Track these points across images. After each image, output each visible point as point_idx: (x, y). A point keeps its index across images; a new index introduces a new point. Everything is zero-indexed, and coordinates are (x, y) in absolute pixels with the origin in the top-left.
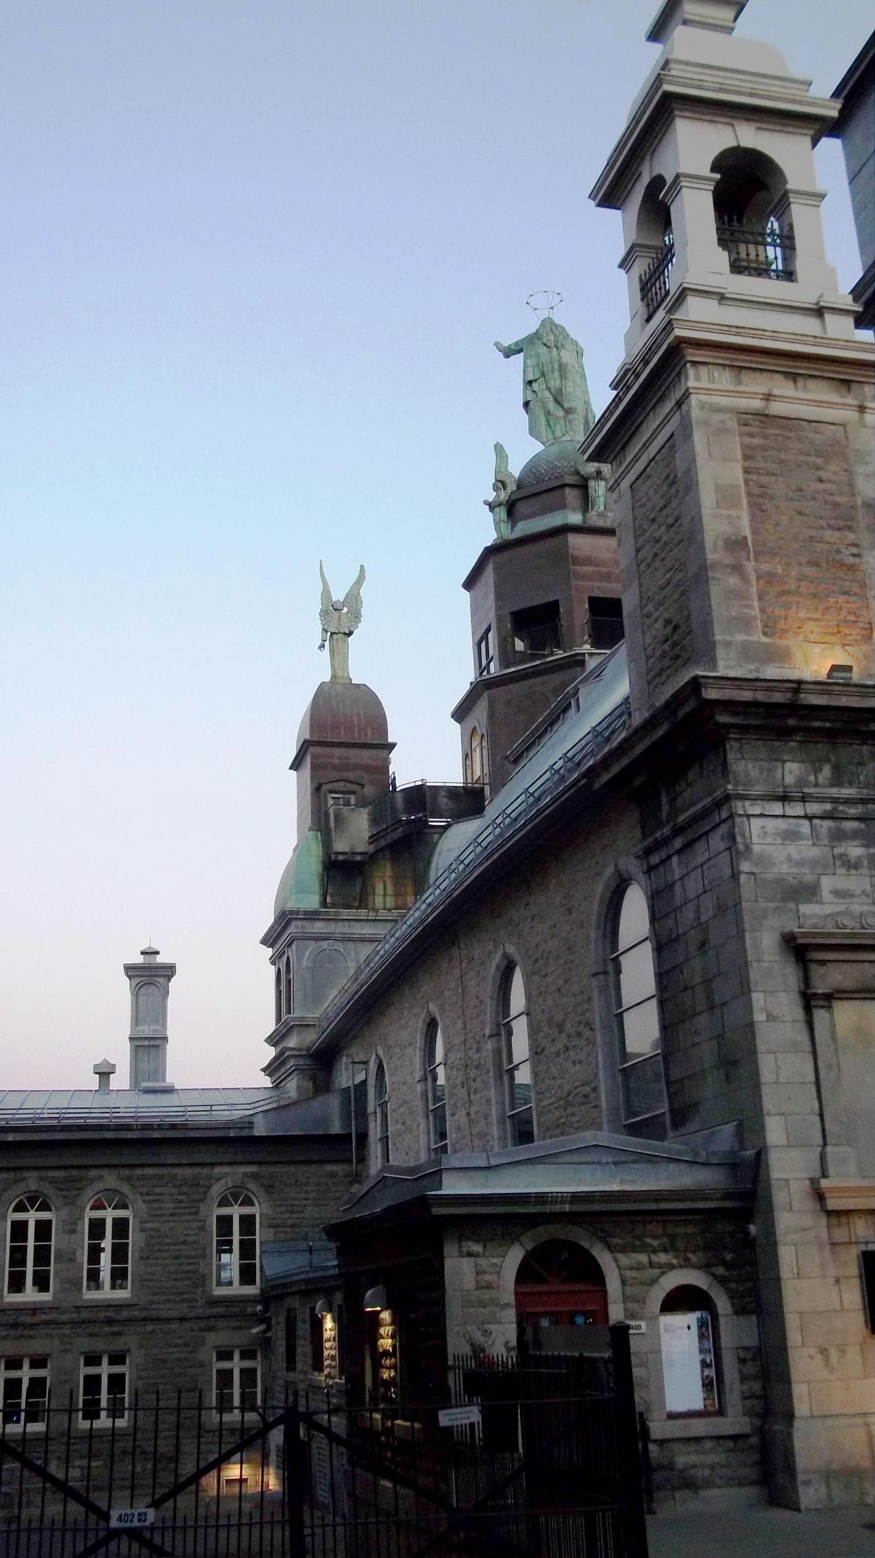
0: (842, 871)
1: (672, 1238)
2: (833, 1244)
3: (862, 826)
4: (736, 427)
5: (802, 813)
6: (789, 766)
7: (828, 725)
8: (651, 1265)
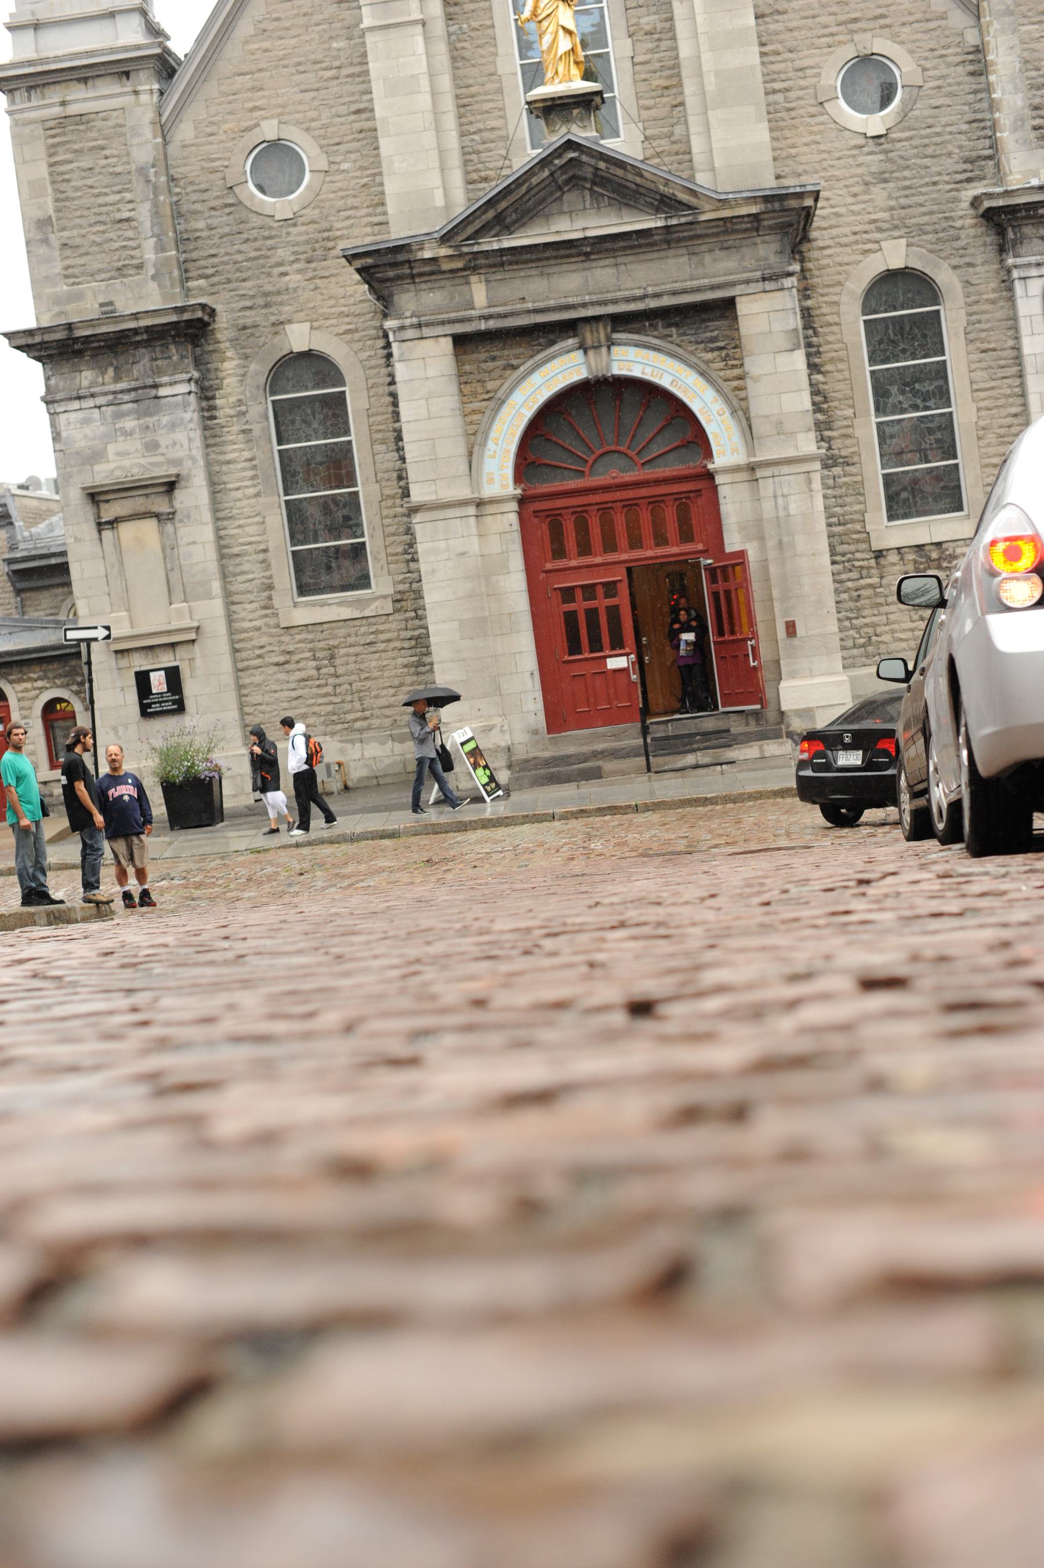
0: (122, 438)
1: (44, 671)
2: (119, 669)
3: (135, 405)
4: (42, 131)
5: (92, 405)
6: (84, 374)
7: (102, 344)
8: (34, 689)
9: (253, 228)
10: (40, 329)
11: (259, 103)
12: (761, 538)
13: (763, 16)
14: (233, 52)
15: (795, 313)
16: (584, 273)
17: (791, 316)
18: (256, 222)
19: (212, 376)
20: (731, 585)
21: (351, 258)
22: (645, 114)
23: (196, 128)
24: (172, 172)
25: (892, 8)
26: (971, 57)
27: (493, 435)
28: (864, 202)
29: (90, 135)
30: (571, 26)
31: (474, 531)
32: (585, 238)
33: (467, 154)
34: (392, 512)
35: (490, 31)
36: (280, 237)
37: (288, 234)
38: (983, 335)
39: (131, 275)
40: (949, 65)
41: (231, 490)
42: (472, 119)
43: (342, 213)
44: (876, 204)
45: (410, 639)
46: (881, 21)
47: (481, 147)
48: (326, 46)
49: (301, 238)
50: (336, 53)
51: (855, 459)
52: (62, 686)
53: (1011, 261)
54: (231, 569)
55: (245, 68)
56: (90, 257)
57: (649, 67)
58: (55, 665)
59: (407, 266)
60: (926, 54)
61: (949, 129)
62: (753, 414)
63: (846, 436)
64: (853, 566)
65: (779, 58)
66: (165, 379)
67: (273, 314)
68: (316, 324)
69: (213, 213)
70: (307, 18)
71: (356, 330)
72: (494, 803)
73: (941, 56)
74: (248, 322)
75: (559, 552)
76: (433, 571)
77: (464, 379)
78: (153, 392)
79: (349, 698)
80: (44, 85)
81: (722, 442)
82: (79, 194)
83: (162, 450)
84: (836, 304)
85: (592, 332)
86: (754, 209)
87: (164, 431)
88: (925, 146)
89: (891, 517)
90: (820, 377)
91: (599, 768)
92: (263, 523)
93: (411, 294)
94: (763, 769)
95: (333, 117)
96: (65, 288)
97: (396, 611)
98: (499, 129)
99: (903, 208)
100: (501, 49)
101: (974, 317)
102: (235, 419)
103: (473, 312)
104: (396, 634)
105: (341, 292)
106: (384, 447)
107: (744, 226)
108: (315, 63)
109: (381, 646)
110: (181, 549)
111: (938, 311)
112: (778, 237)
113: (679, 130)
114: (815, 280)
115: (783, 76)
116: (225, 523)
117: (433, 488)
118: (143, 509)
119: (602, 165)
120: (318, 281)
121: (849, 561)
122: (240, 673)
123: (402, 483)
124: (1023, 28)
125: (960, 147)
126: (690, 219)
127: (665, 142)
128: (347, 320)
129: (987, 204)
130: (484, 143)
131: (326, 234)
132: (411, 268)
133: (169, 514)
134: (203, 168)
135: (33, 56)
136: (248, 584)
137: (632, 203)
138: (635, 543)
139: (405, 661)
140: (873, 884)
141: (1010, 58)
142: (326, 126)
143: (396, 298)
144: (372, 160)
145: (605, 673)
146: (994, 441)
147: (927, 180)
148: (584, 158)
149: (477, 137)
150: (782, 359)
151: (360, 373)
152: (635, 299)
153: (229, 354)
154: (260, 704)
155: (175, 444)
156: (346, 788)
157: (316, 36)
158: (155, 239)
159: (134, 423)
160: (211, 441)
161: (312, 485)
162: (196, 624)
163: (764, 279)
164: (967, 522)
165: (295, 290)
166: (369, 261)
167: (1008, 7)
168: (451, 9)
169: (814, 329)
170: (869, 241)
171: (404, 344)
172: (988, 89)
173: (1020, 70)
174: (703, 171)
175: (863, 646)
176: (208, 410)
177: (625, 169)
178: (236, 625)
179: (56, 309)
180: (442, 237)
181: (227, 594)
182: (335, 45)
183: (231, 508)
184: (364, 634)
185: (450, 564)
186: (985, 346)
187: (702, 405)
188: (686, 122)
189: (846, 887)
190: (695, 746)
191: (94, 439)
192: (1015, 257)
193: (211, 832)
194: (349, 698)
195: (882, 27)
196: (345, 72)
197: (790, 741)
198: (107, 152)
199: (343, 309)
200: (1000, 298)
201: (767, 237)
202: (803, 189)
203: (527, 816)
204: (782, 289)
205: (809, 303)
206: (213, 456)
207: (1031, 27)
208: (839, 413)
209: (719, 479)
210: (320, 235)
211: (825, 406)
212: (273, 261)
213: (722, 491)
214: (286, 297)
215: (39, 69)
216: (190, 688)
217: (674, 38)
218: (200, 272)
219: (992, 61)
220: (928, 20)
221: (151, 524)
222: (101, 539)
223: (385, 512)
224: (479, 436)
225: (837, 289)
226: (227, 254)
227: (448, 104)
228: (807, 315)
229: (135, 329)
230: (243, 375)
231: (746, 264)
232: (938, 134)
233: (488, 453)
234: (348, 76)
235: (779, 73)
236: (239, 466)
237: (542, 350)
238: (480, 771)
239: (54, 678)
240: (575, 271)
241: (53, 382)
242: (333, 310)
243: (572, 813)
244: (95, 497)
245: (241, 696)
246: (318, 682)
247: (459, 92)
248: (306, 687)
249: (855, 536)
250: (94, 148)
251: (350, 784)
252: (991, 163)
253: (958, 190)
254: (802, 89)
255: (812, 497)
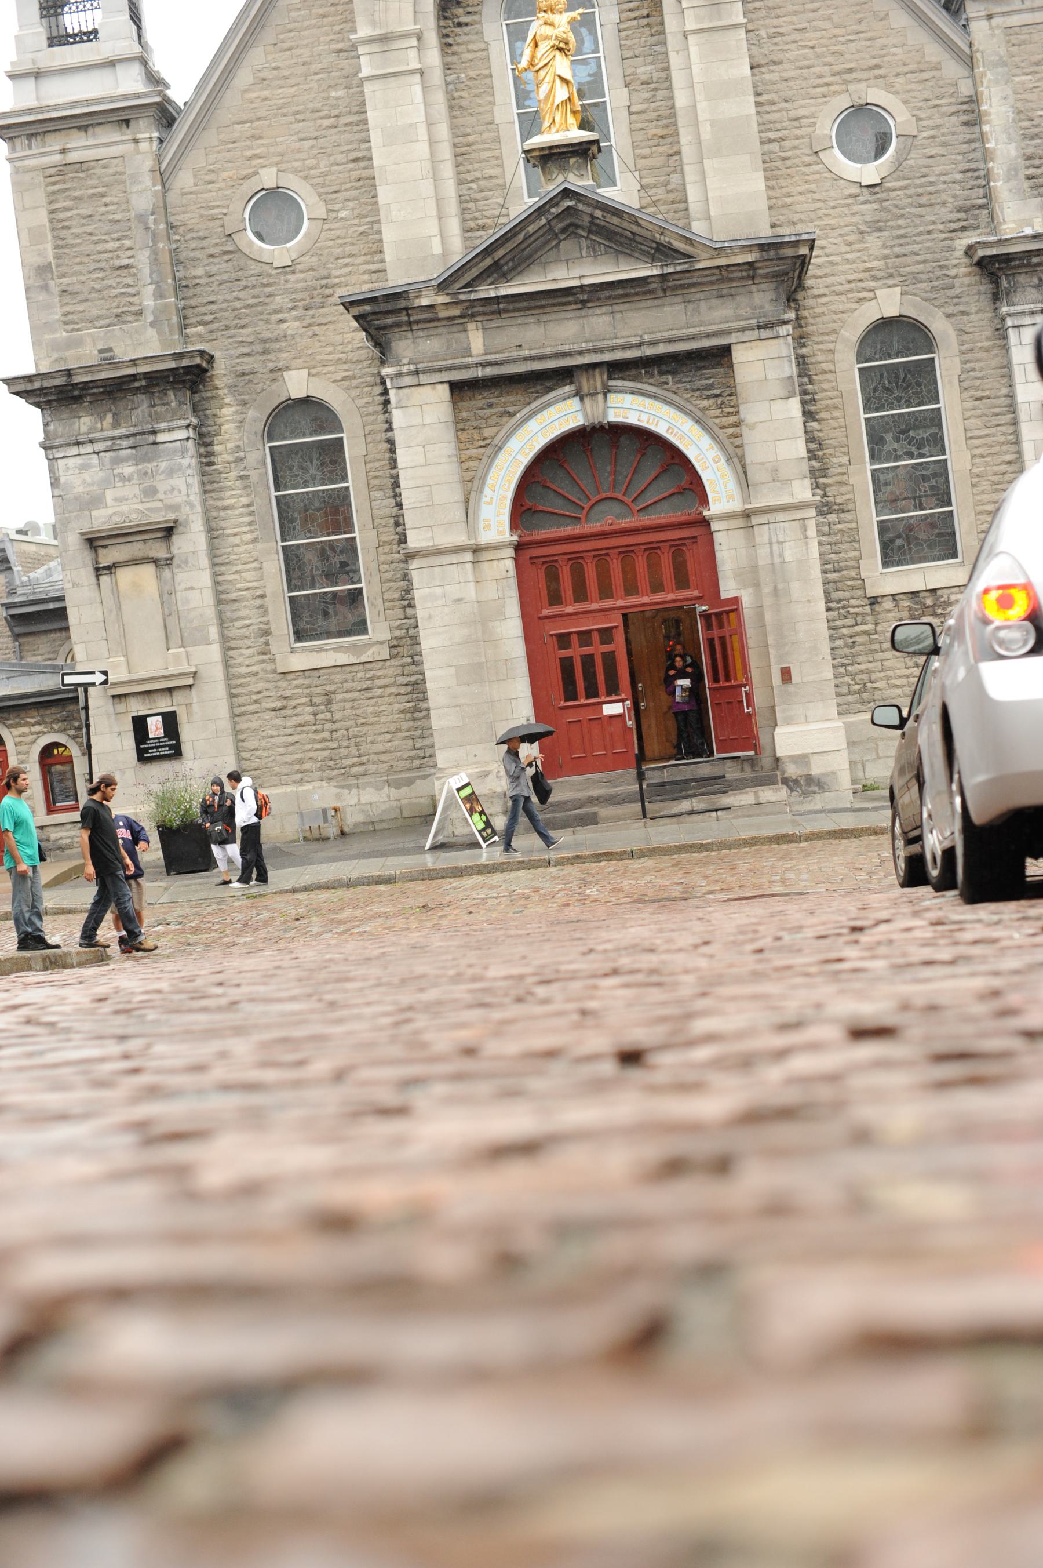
0: (120, 484)
3: (134, 451)
4: (42, 179)
6: (82, 420)
9: (252, 276)
10: (39, 375)
11: (258, 151)
12: (757, 585)
13: (759, 66)
14: (232, 101)
15: (790, 361)
16: (581, 321)
17: (786, 364)
18: (255, 269)
19: (210, 422)
20: (726, 631)
21: (349, 305)
22: (642, 163)
23: (195, 176)
24: (171, 219)
25: (886, 59)
26: (964, 107)
27: (489, 481)
28: (859, 251)
29: (90, 182)
30: (568, 75)
31: (471, 578)
32: (581, 286)
33: (464, 202)
34: (389, 558)
35: (487, 81)
36: (279, 284)
37: (286, 281)
38: (978, 382)
39: (130, 322)
40: (943, 115)
41: (228, 536)
42: (470, 167)
43: (340, 261)
44: (871, 252)
45: (407, 685)
46: (876, 71)
47: (478, 196)
48: (325, 95)
49: (299, 285)
50: (335, 102)
51: (850, 506)
52: (59, 731)
53: (1004, 309)
54: (229, 614)
55: (245, 117)
56: (89, 303)
57: (644, 116)
58: (53, 710)
59: (405, 313)
60: (920, 104)
61: (942, 178)
62: (748, 461)
63: (842, 483)
64: (848, 612)
65: (774, 108)
66: (163, 425)
67: (271, 361)
68: (313, 371)
69: (212, 260)
70: (306, 67)
71: (354, 377)
72: (489, 849)
73: (936, 106)
74: (247, 368)
75: (555, 598)
76: (430, 617)
77: (461, 426)
78: (151, 438)
79: (345, 743)
80: (45, 132)
81: (717, 489)
82: (79, 241)
83: (160, 496)
84: (832, 351)
85: (588, 378)
86: (750, 258)
87: (162, 477)
88: (919, 195)
89: (886, 564)
90: (815, 425)
91: (595, 814)
92: (261, 568)
93: (409, 341)
94: (758, 815)
95: (332, 165)
96: (64, 334)
97: (393, 657)
98: (496, 177)
99: (897, 256)
100: (499, 98)
101: (968, 365)
102: (233, 465)
103: (469, 360)
104: (393, 679)
105: (339, 338)
106: (381, 493)
107: (740, 274)
108: (313, 112)
109: (379, 692)
110: (179, 594)
111: (933, 359)
112: (773, 285)
113: (675, 179)
114: (810, 329)
115: (778, 126)
116: (223, 568)
117: (430, 534)
118: (141, 555)
119: (598, 213)
120: (316, 328)
121: (843, 607)
122: (237, 719)
123: (399, 529)
124: (1017, 79)
125: (955, 196)
126: (685, 267)
127: (661, 190)
128: (345, 366)
129: (981, 253)
130: (481, 191)
131: (324, 282)
132: (408, 315)
133: (167, 559)
134: (202, 216)
135: (33, 103)
136: (244, 630)
137: (628, 251)
138: (631, 589)
139: (402, 706)
140: (867, 931)
141: (1003, 109)
142: (323, 175)
143: (393, 344)
144: (370, 208)
145: (600, 719)
146: (989, 488)
147: (921, 229)
148: (580, 207)
149: (474, 186)
150: (777, 406)
151: (357, 420)
152: (630, 347)
153: (227, 401)
154: (257, 749)
155: (173, 489)
156: (342, 833)
157: (315, 85)
158: (154, 286)
159: (132, 469)
160: (209, 487)
161: (310, 531)
162: (193, 669)
163: (759, 327)
164: (961, 569)
165: (293, 337)
166: (367, 308)
167: (1001, 57)
168: (449, 59)
169: (809, 377)
170: (864, 289)
171: (401, 391)
172: (982, 138)
173: (1014, 120)
174: (699, 220)
175: (858, 692)
176: (206, 457)
177: (622, 218)
178: (233, 670)
179: (55, 355)
180: (439, 284)
181: (224, 639)
182: (333, 94)
183: (229, 554)
184: (361, 680)
185: (446, 610)
186: (979, 394)
187: (697, 452)
188: (682, 172)
189: (839, 935)
190: (690, 792)
191: (93, 484)
193: (208, 877)
194: (345, 743)
195: (876, 77)
196: (344, 120)
197: (785, 787)
198: (107, 200)
199: (341, 356)
200: (995, 345)
201: (762, 286)
202: (798, 238)
203: (523, 862)
204: (777, 337)
205: (804, 351)
206: (211, 502)
207: (1024, 78)
208: (834, 460)
209: (715, 526)
210: (318, 283)
211: (820, 453)
212: (272, 307)
213: (718, 538)
214: (284, 344)
215: (40, 117)
216: (186, 733)
217: (670, 88)
218: (198, 319)
219: (986, 111)
220: (922, 71)
221: (149, 570)
222: (99, 585)
223: (382, 558)
224: (476, 482)
225: (832, 337)
226: (226, 301)
227: (446, 152)
228: (802, 361)
229: (134, 375)
230: (241, 422)
231: (742, 312)
232: (931, 183)
233: (484, 499)
234: (346, 125)
235: (774, 122)
236: (237, 512)
237: (538, 397)
238: (476, 816)
239: (52, 722)
240: (571, 318)
241: (52, 427)
242: (331, 357)
243: (568, 859)
244: (93, 542)
245: (238, 741)
246: (314, 728)
247: (457, 140)
248: (302, 732)
249: (849, 583)
250: (94, 195)
251: (346, 829)
252: (985, 212)
253: (952, 239)
254: (798, 138)
255: (807, 544)
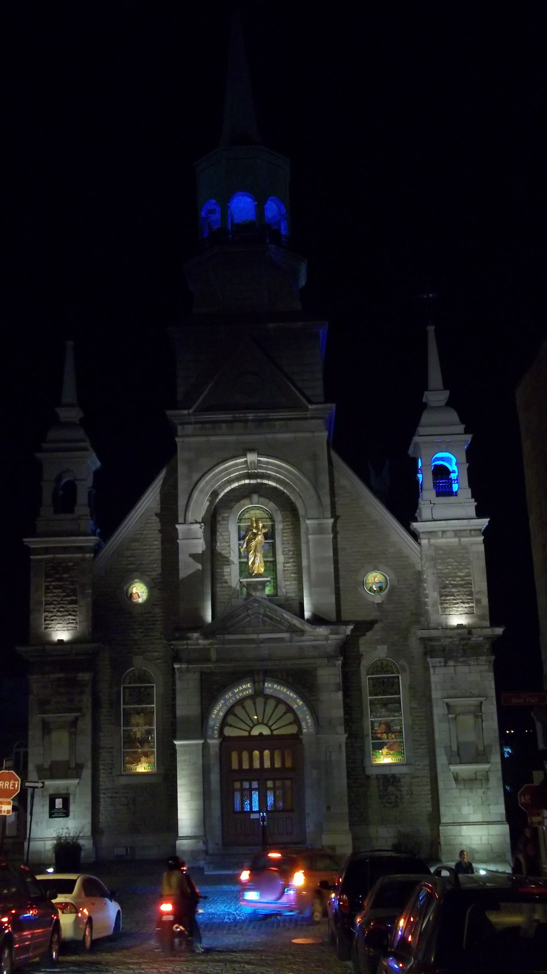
15: (340, 676)
17: (338, 678)
192: (431, 657)
204: (335, 666)
216: (72, 808)
